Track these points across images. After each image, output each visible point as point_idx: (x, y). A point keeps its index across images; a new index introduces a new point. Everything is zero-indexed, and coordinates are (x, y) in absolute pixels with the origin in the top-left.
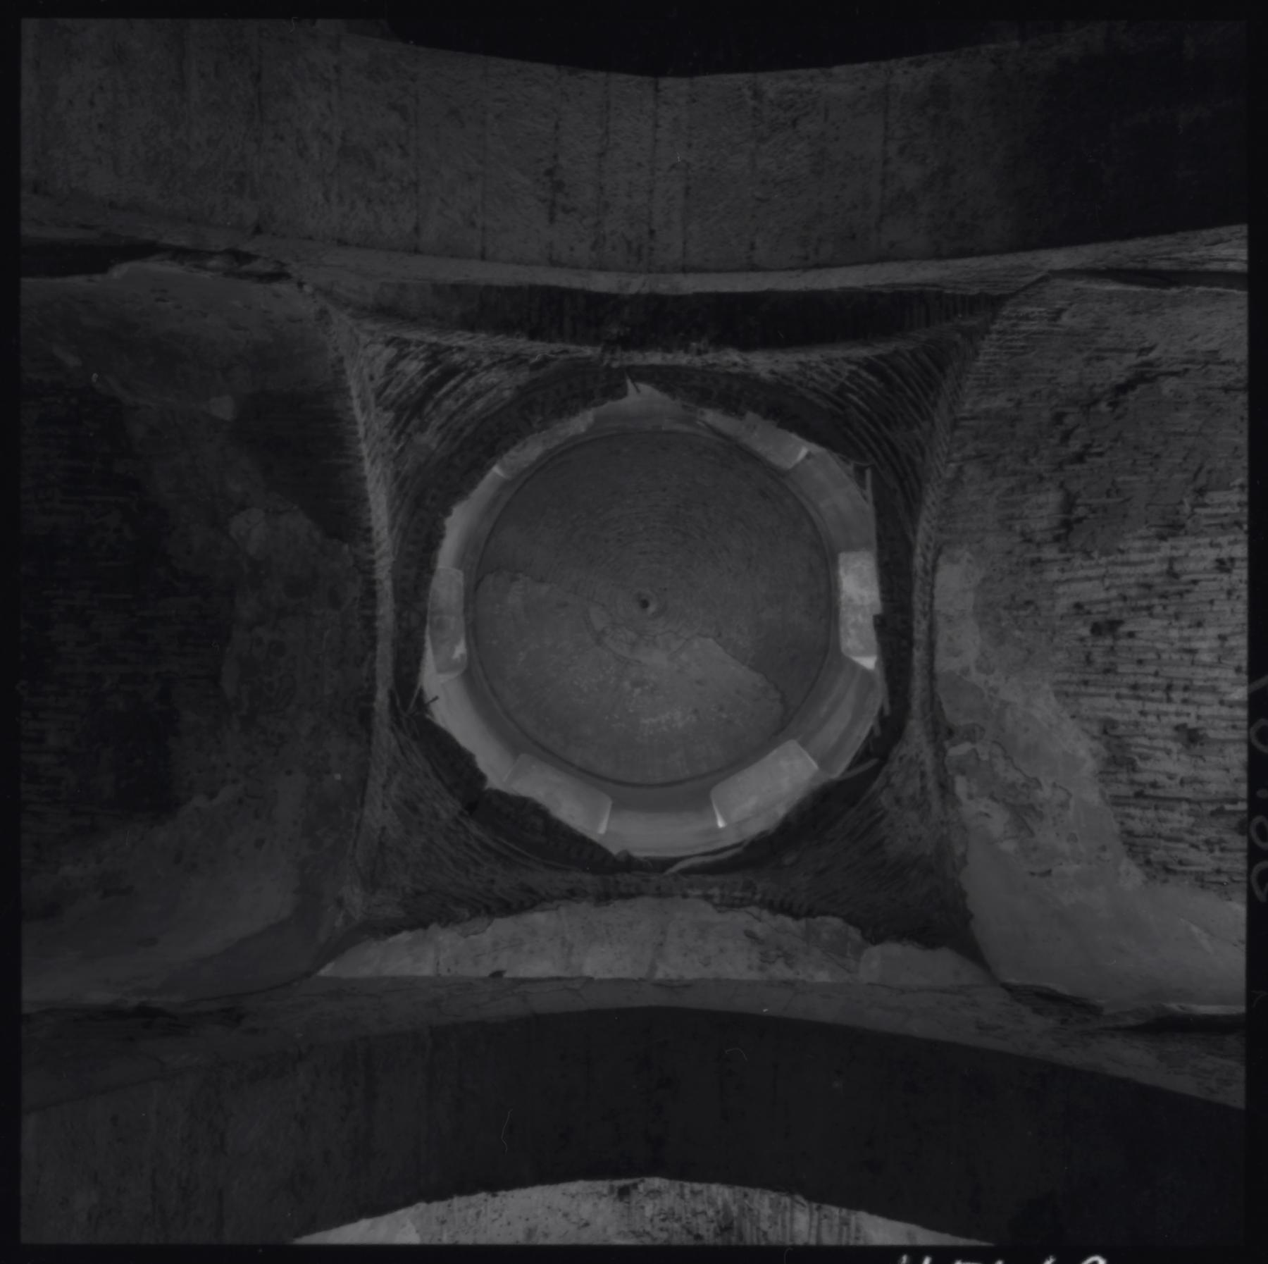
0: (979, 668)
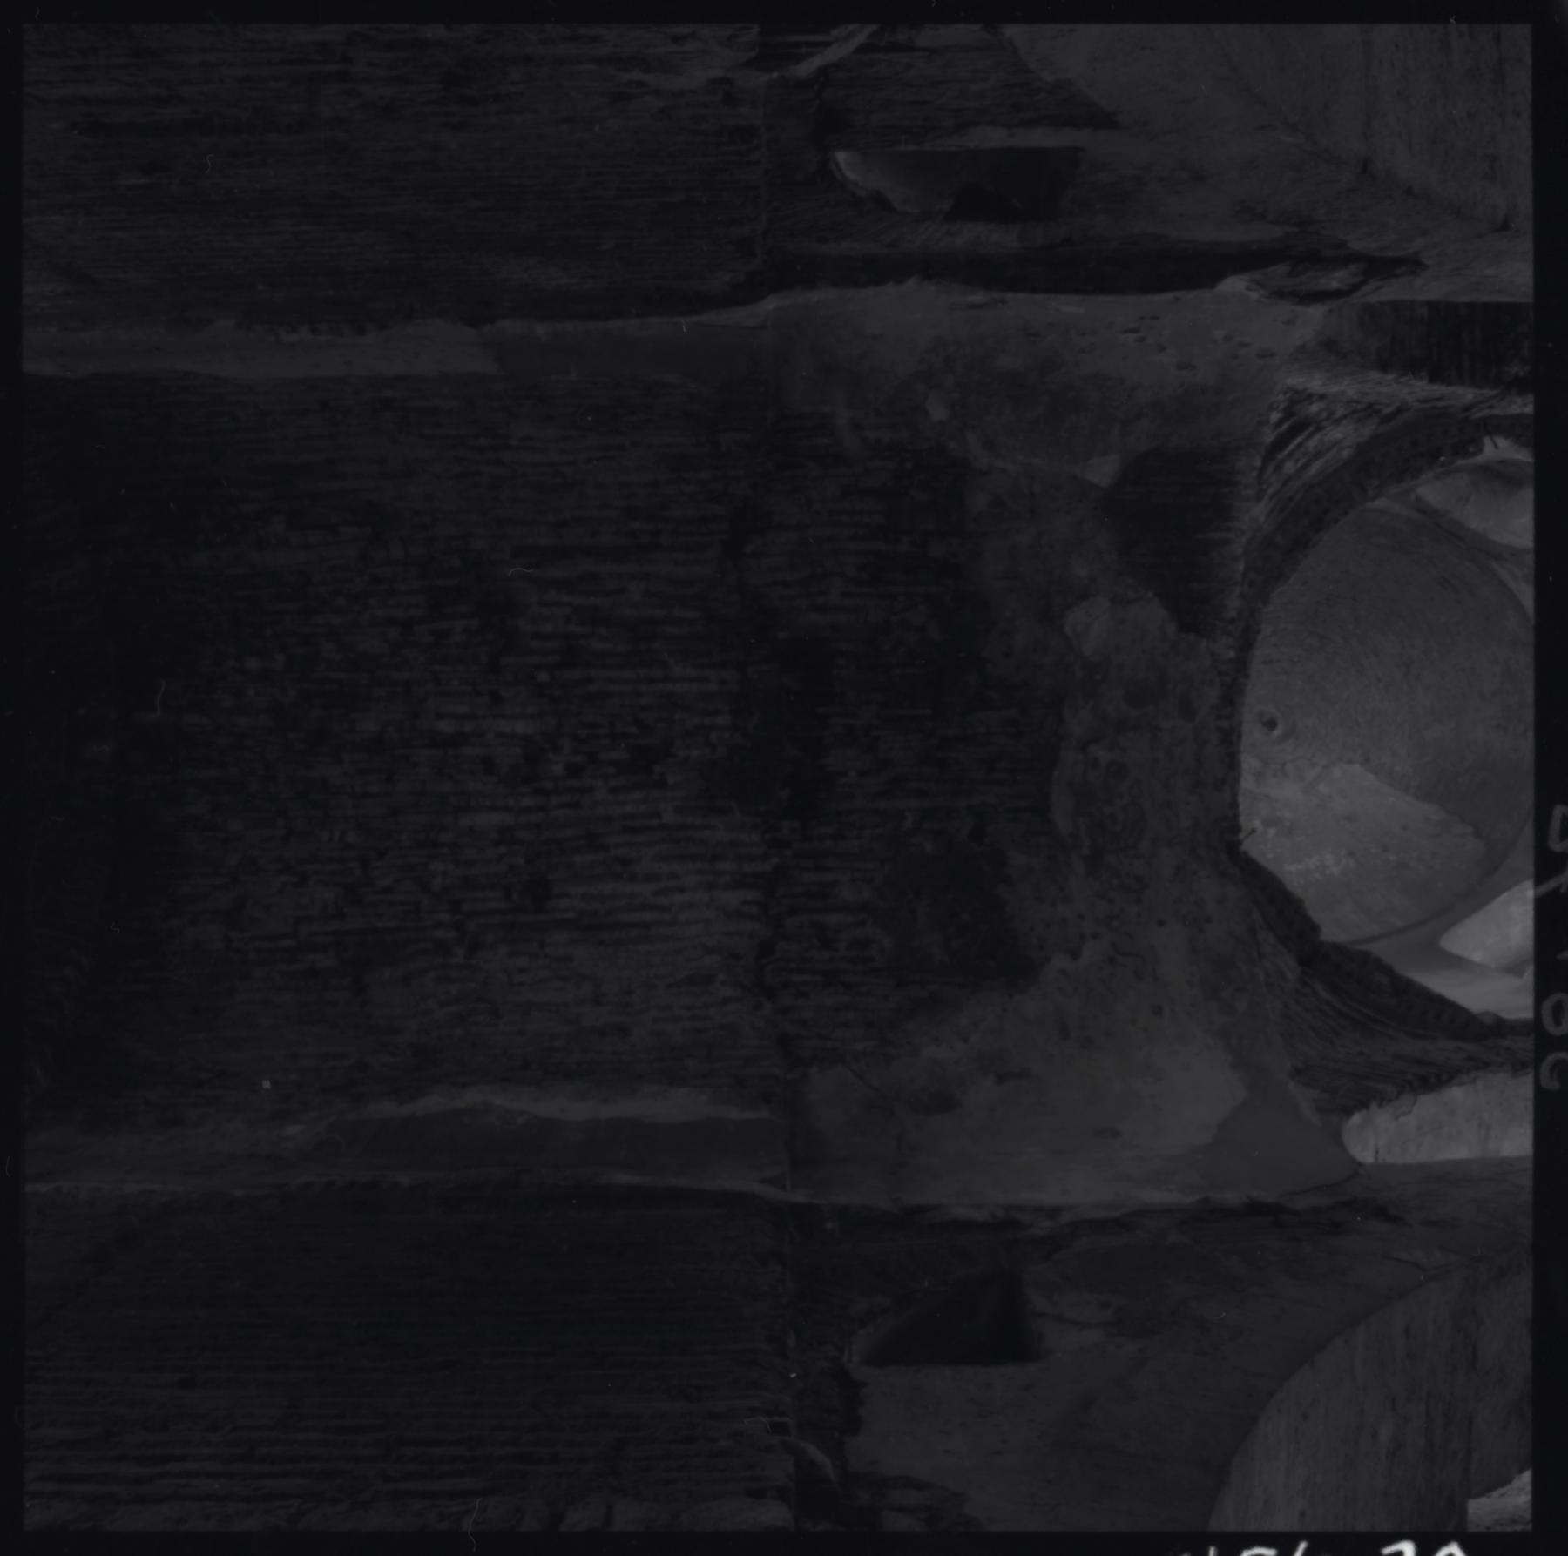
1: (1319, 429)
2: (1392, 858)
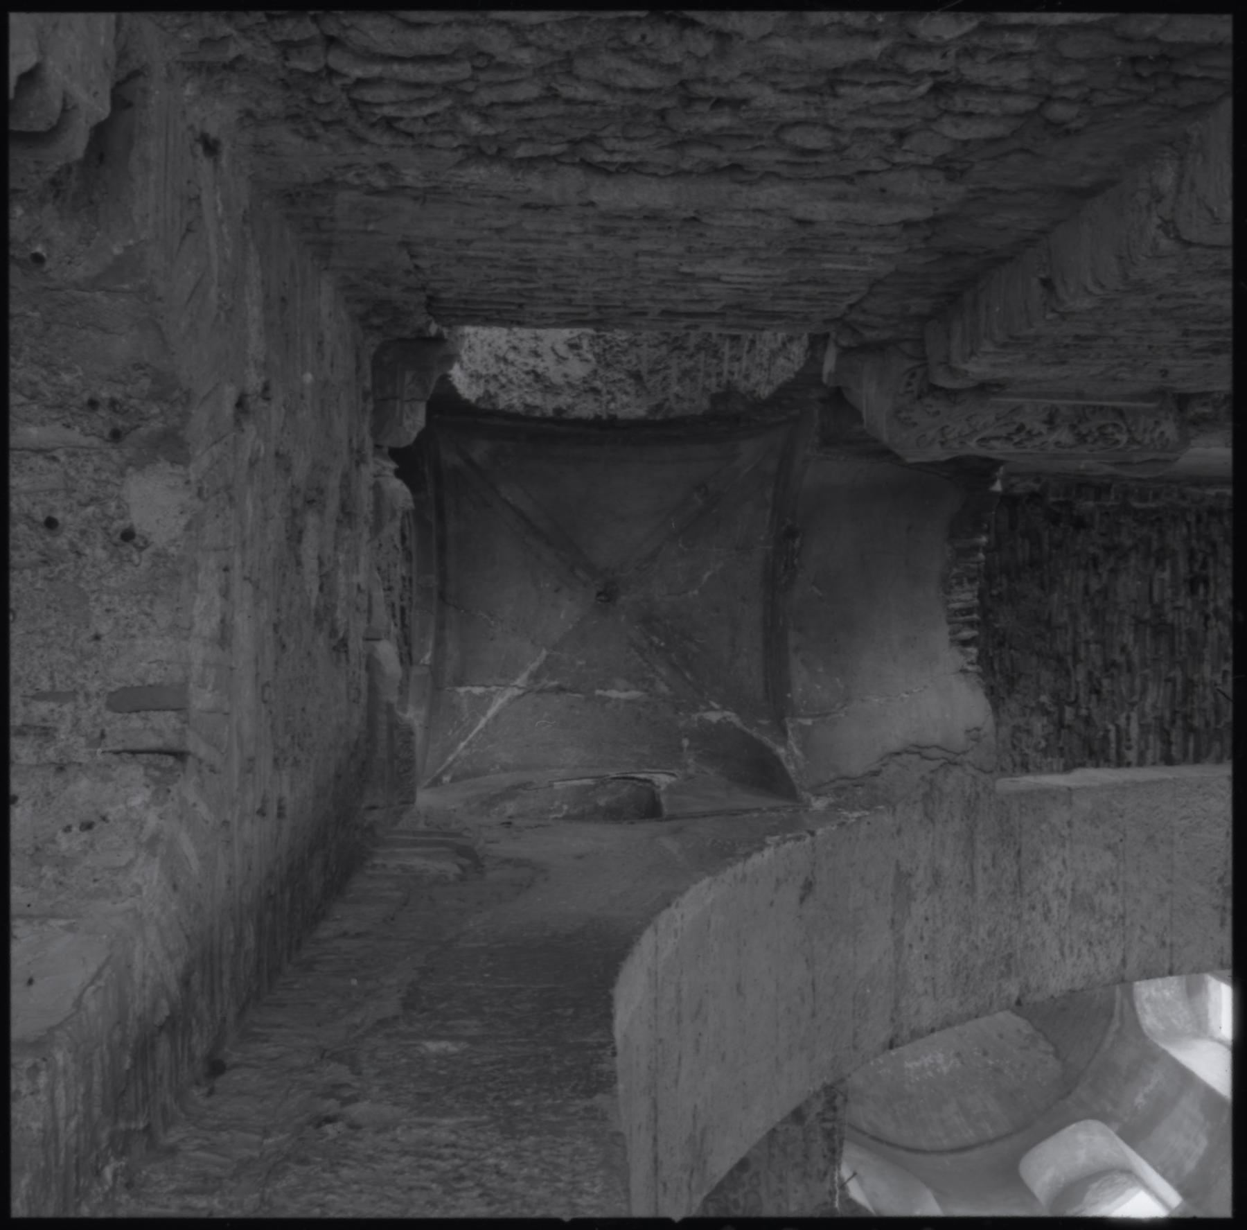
2: (991, 1062)
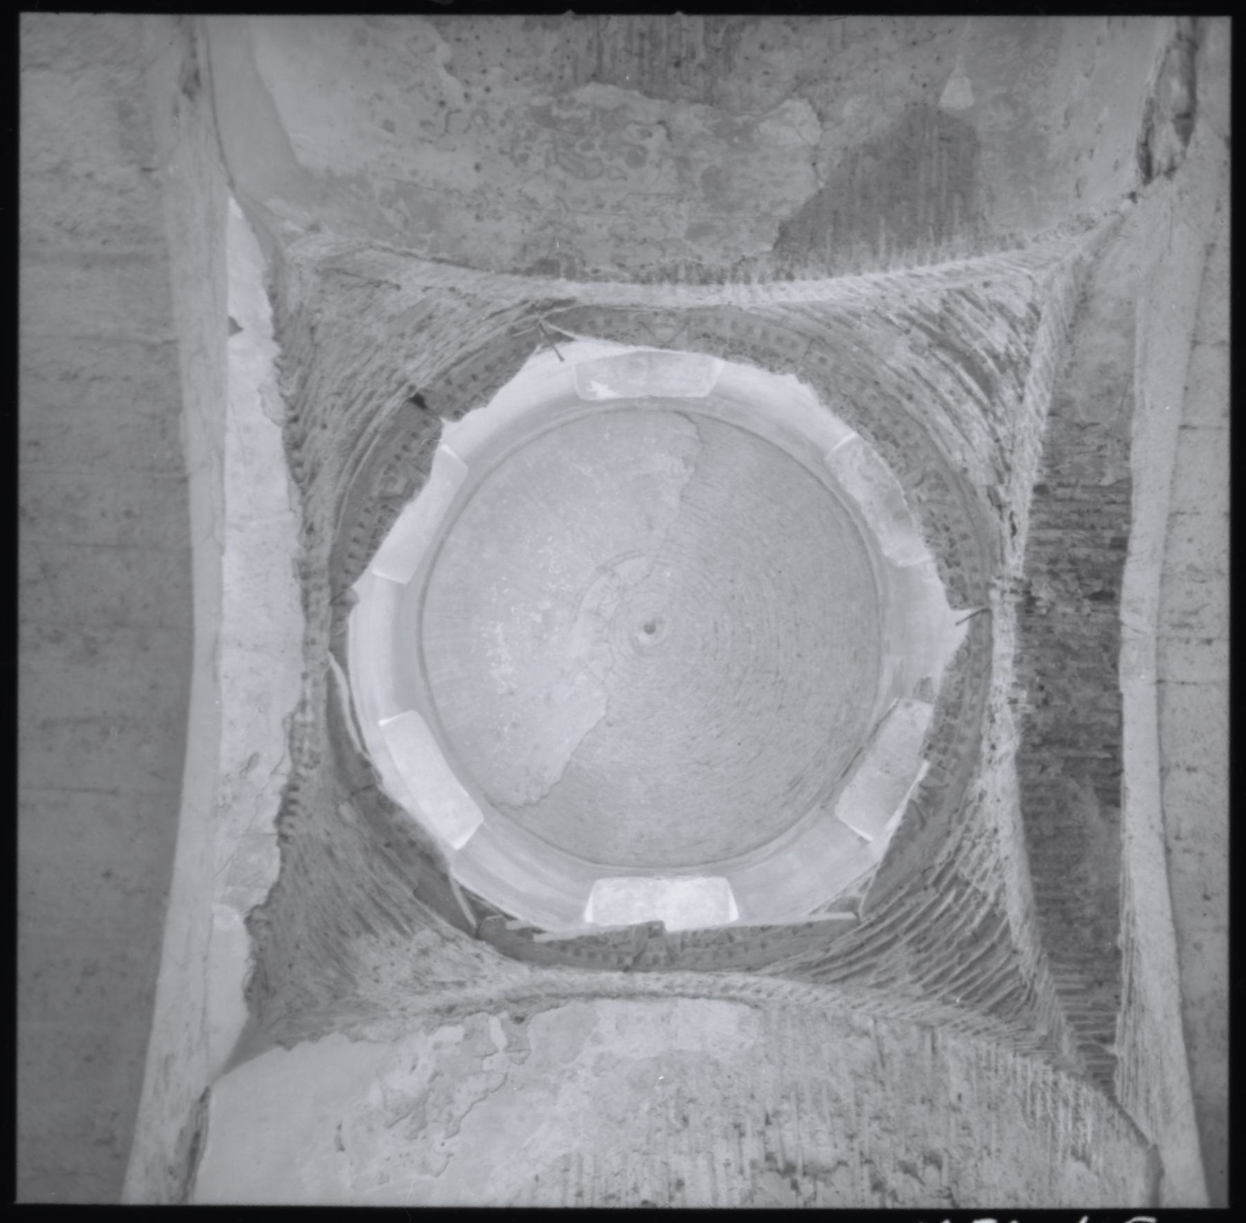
0: (601, 1057)
1: (985, 411)
2: (506, 729)
